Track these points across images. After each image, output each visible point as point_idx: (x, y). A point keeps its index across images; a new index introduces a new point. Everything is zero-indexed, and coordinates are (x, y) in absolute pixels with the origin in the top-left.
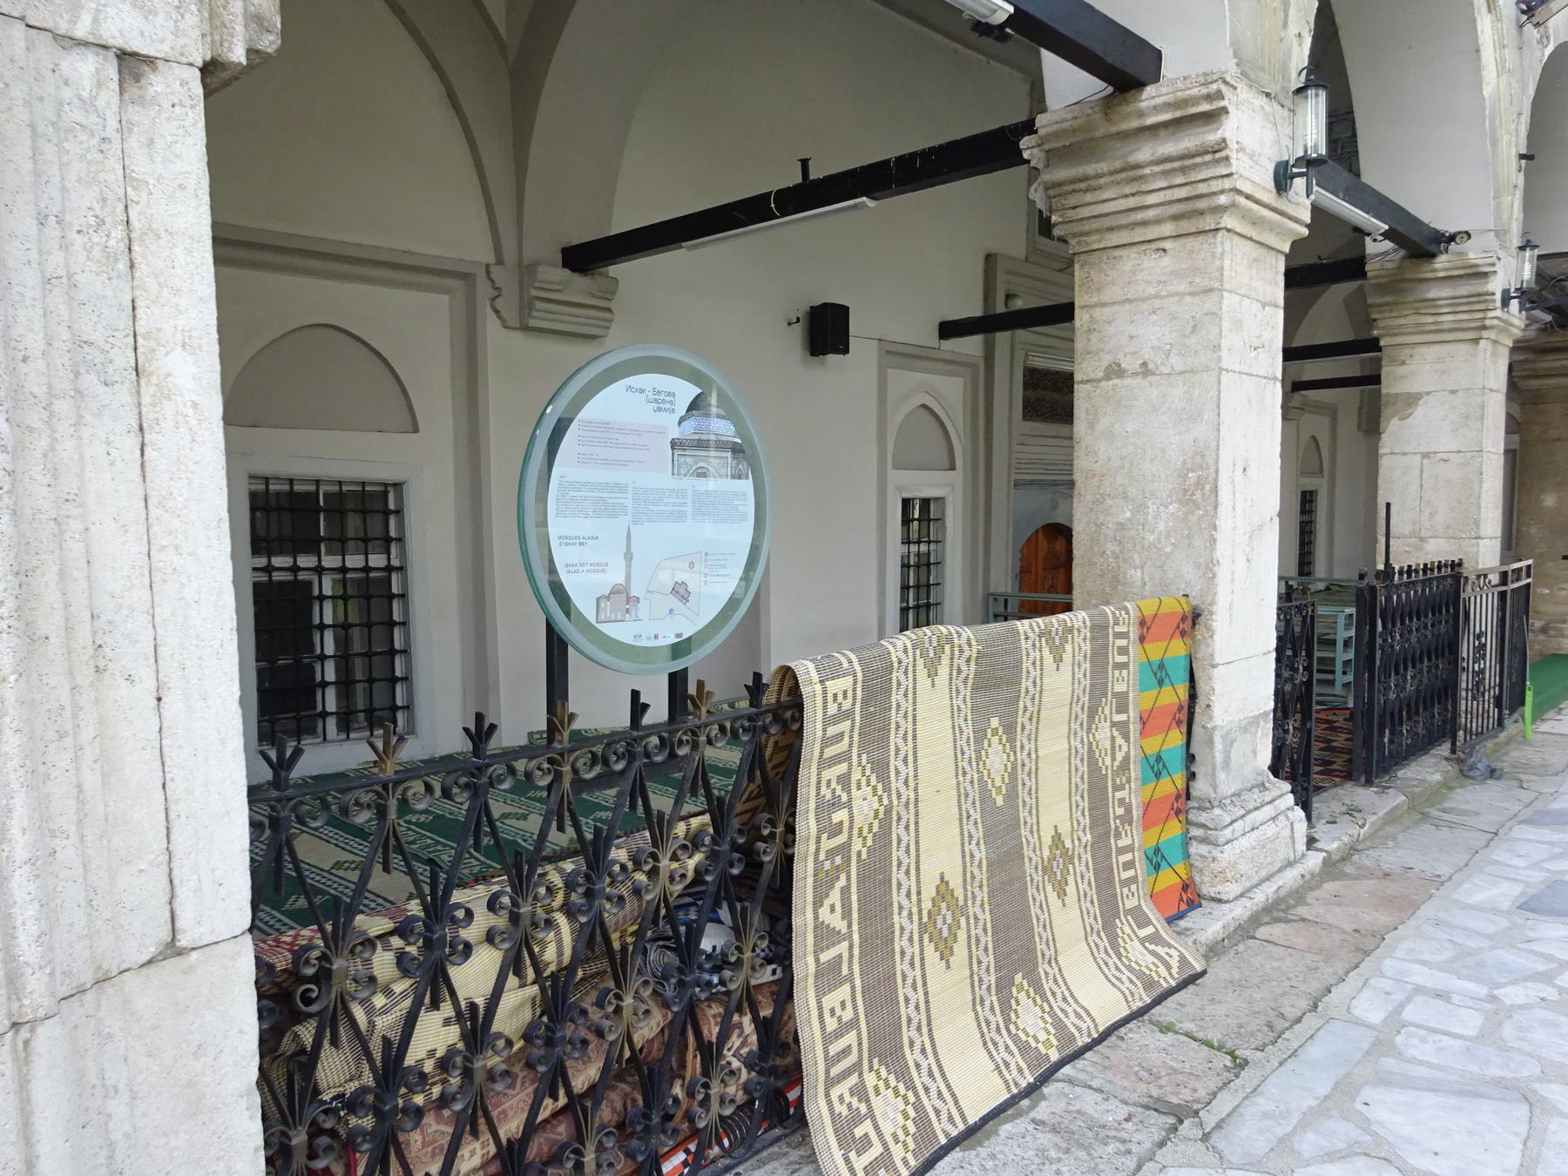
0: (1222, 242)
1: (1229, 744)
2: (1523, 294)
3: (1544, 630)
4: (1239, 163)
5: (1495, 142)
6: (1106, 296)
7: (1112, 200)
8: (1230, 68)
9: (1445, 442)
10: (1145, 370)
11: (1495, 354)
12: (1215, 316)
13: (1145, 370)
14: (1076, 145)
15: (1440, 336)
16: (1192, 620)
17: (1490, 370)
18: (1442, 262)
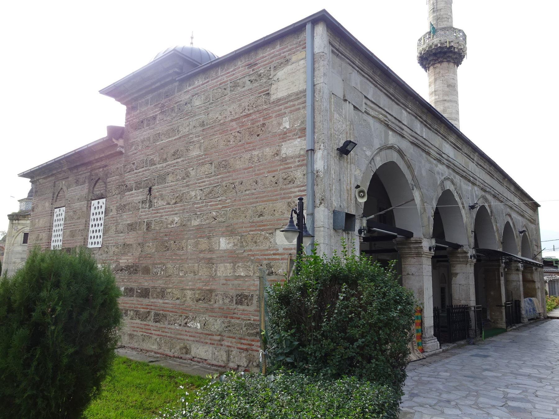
0: (423, 258)
1: (427, 330)
2: (474, 256)
3: (494, 322)
4: (424, 248)
5: (467, 230)
6: (407, 263)
7: (407, 251)
8: (422, 237)
9: (463, 282)
10: (413, 274)
11: (471, 266)
12: (422, 268)
13: (413, 274)
14: (401, 243)
15: (461, 262)
16: (421, 311)
17: (470, 270)
18: (459, 250)
